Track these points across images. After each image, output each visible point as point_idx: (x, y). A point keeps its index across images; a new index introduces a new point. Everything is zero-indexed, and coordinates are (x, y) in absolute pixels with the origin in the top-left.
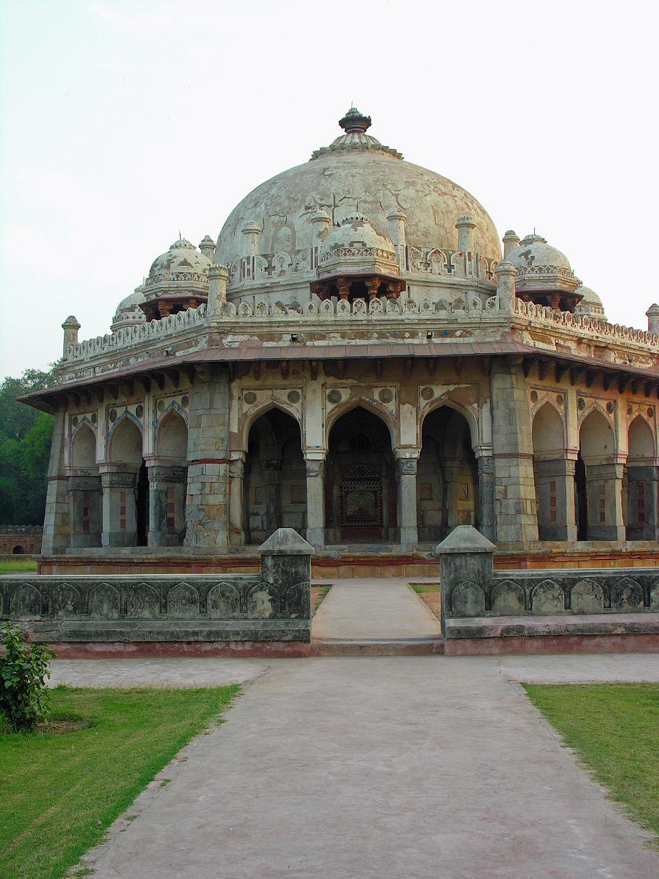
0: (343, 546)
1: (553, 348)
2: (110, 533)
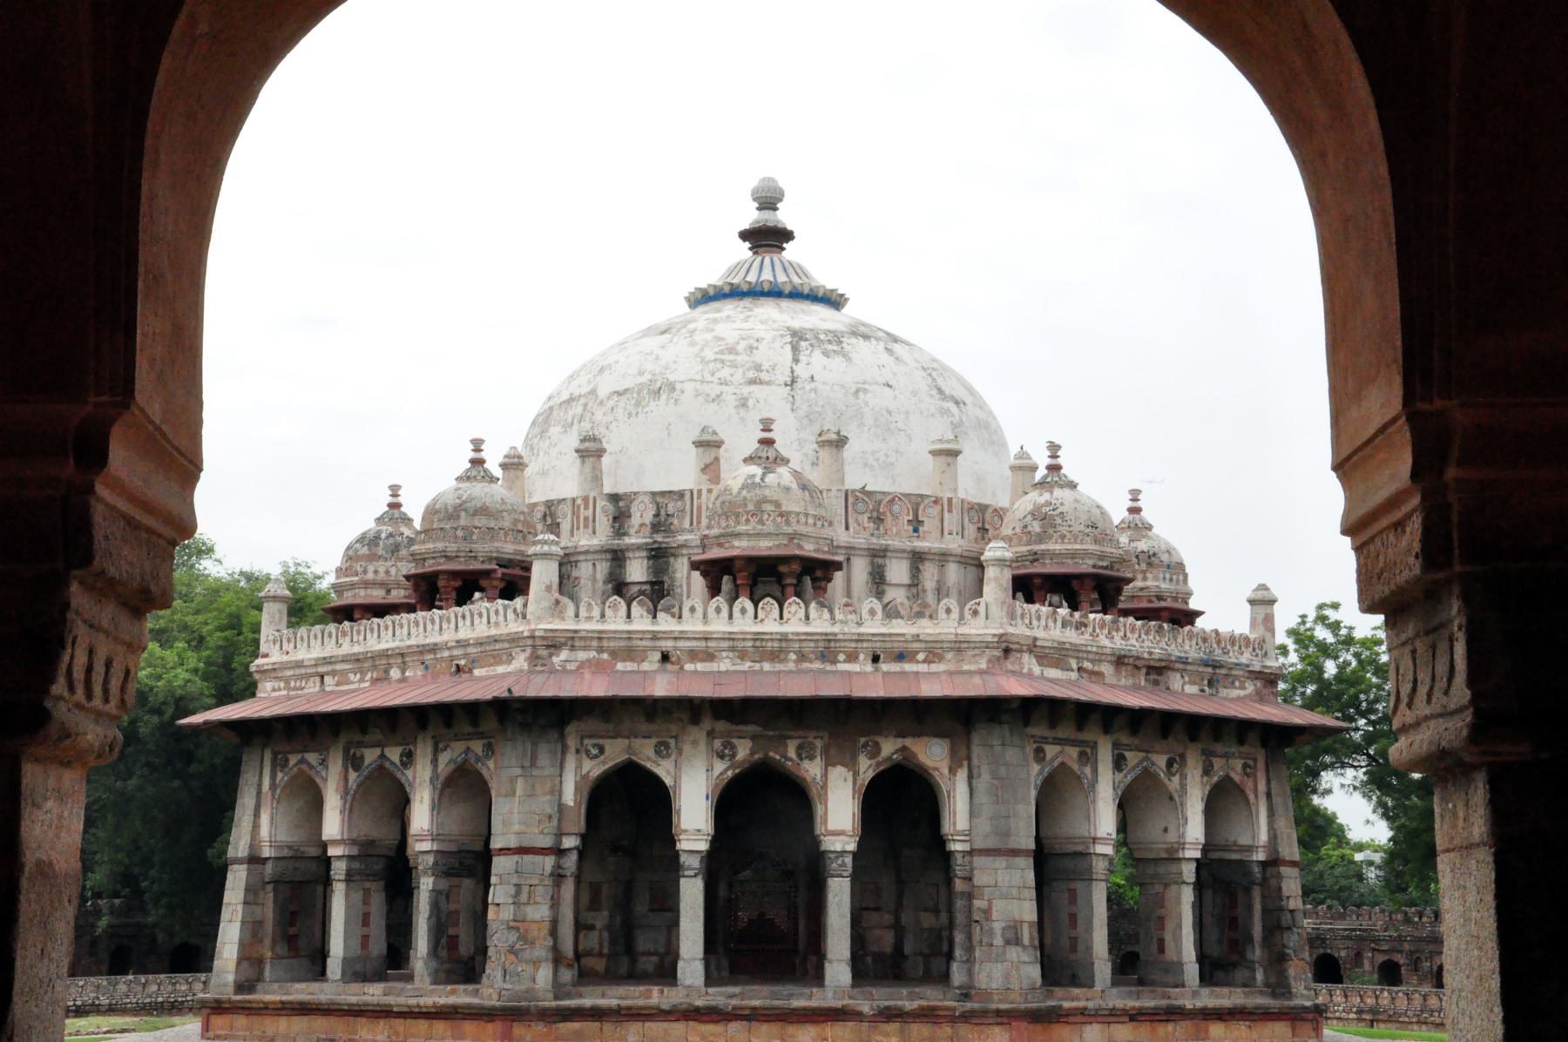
0: (736, 990)
2: (346, 961)
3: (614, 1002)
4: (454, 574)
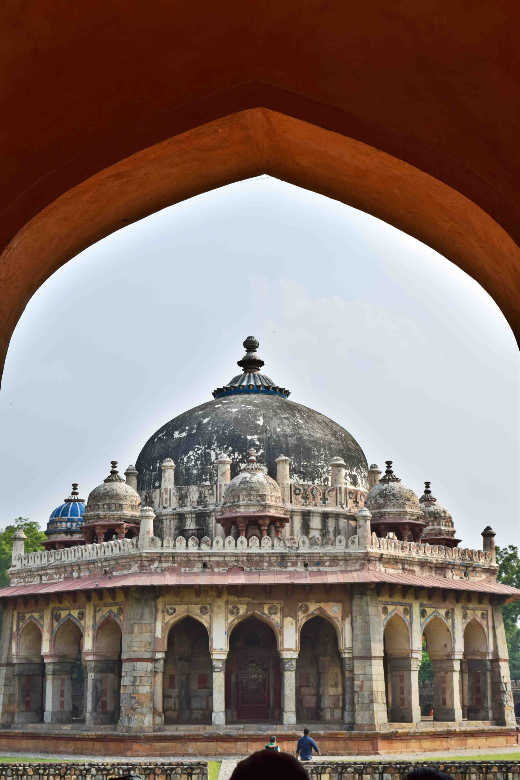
0: (242, 726)
2: (53, 713)
3: (182, 733)
4: (103, 526)
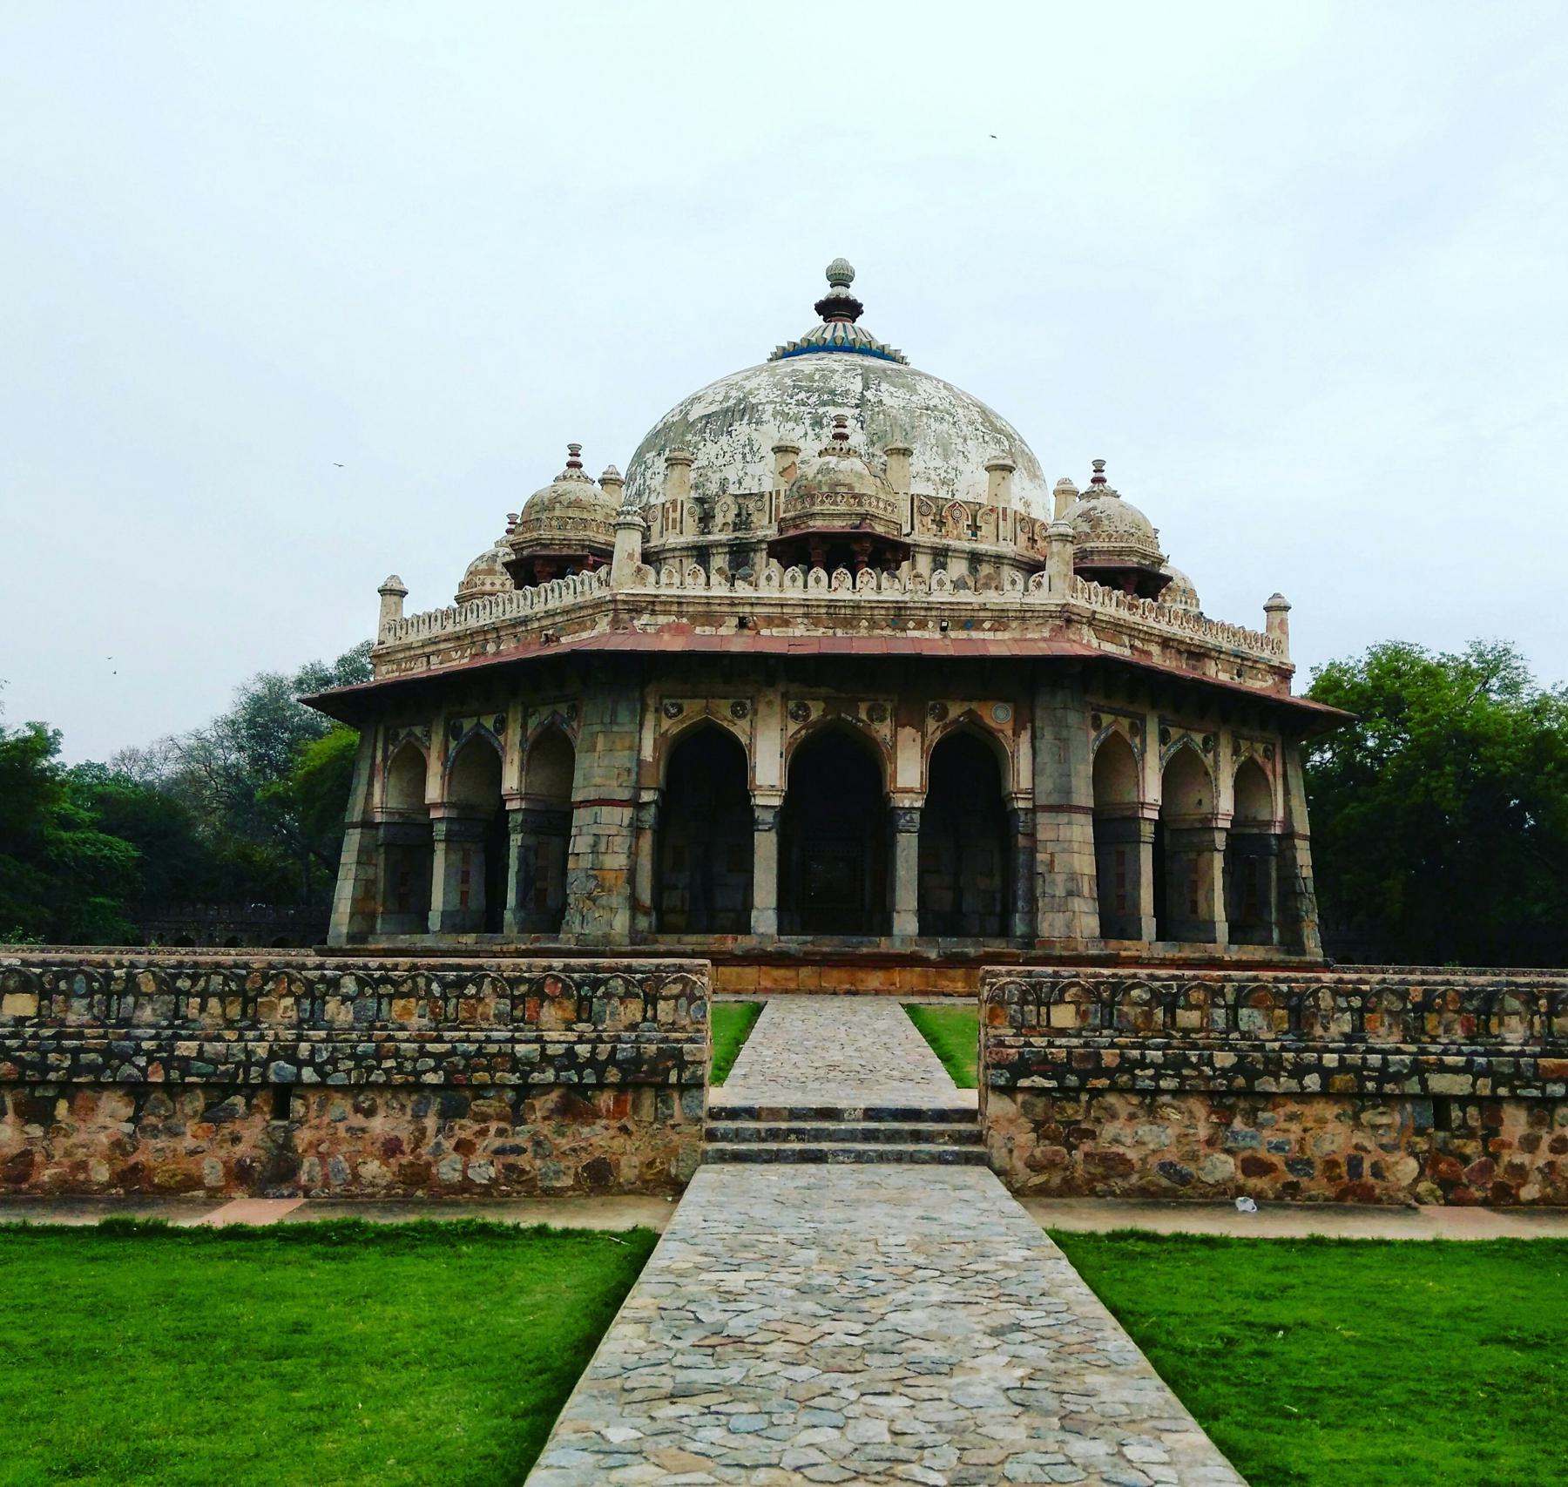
0: (809, 938)
1: (1127, 652)
